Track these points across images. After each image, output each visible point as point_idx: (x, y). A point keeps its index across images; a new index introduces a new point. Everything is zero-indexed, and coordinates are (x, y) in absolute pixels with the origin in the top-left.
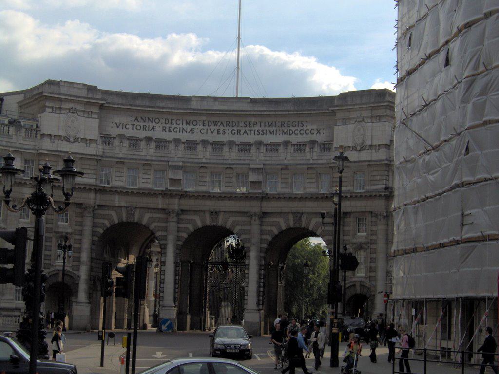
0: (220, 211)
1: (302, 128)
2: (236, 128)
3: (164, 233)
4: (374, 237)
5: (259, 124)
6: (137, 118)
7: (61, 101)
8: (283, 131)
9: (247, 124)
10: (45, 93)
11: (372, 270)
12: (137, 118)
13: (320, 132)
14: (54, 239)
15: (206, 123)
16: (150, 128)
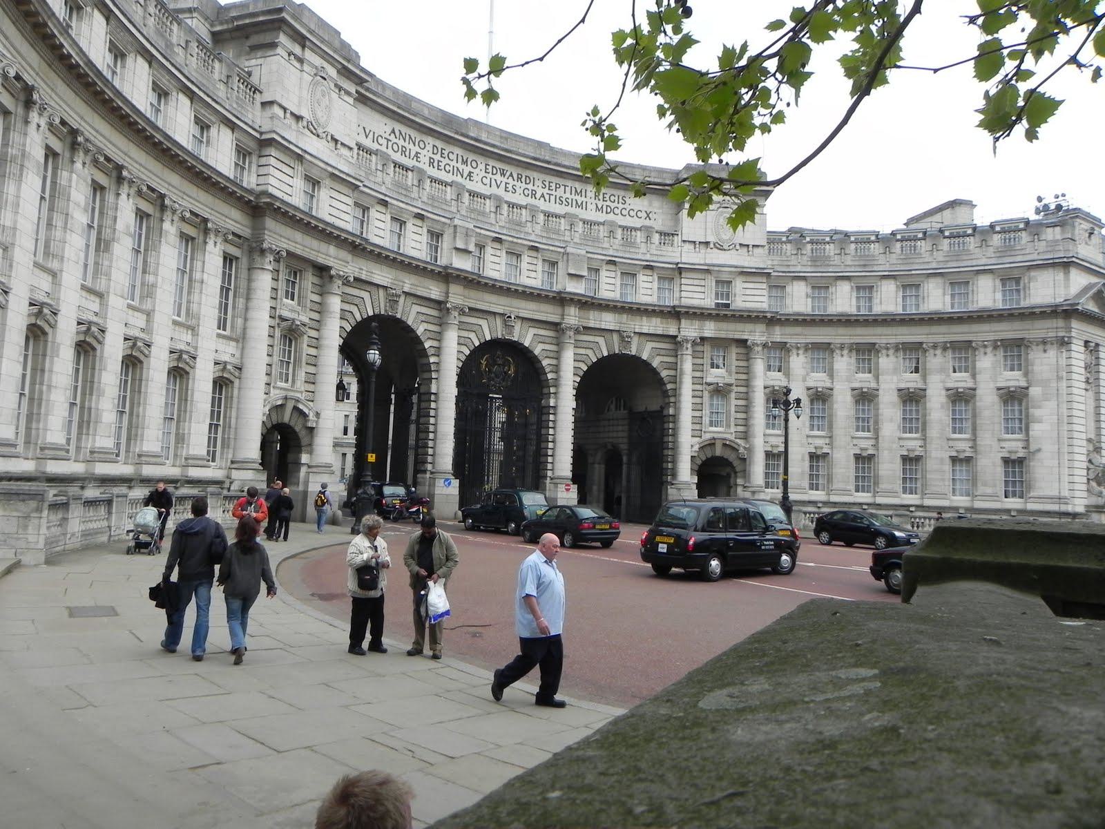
0: (518, 317)
1: (625, 206)
2: (530, 186)
3: (435, 344)
4: (744, 377)
5: (563, 187)
6: (393, 130)
7: (303, 47)
8: (597, 207)
9: (547, 184)
10: (288, 13)
11: (747, 422)
12: (393, 130)
13: (650, 215)
14: (278, 333)
15: (490, 168)
16: (412, 155)
